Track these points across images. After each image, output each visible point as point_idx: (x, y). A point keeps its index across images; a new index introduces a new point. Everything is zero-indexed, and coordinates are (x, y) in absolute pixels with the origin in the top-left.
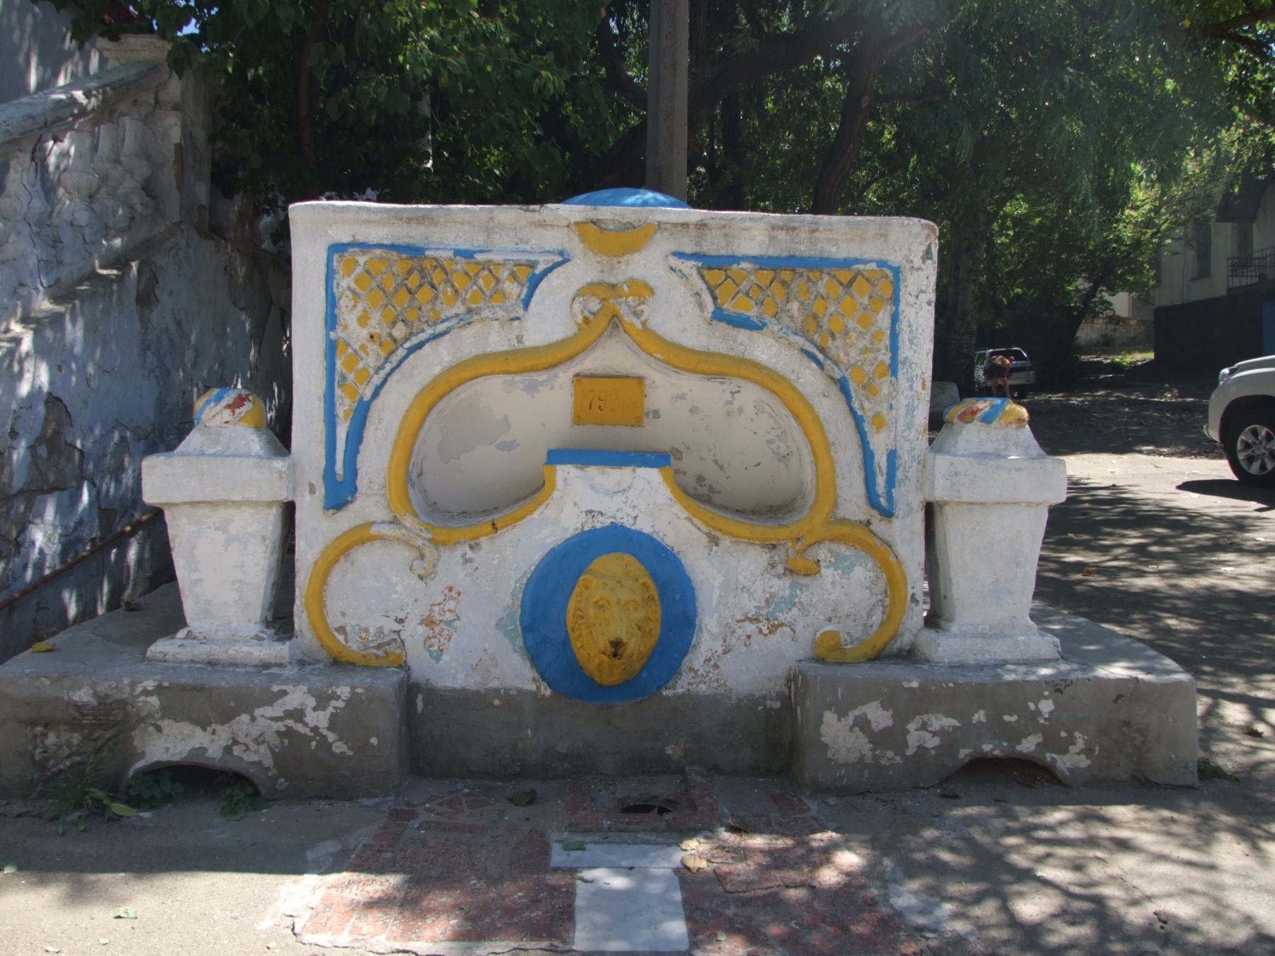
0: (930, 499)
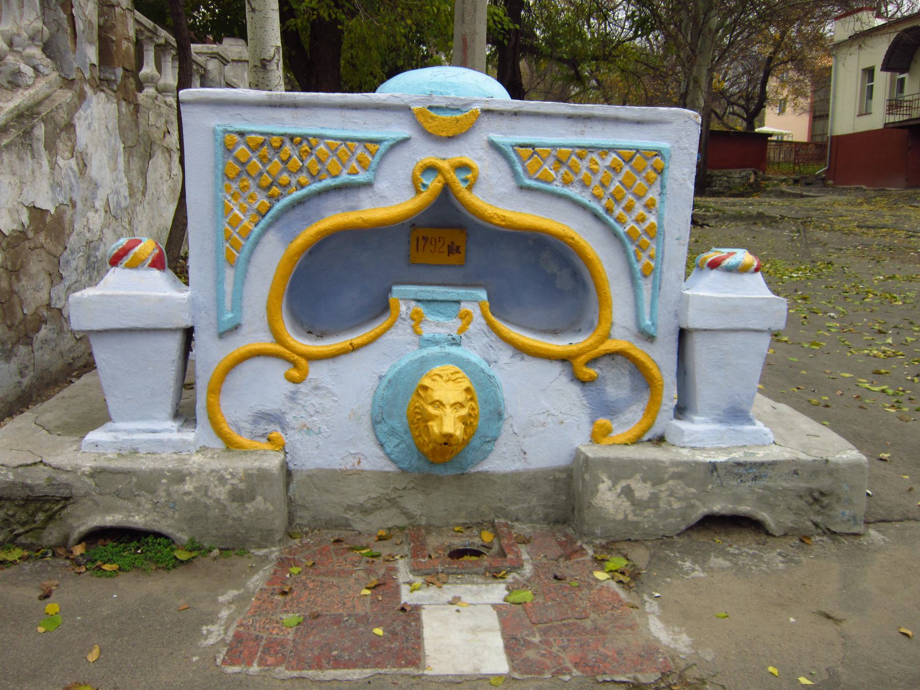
0: (684, 326)
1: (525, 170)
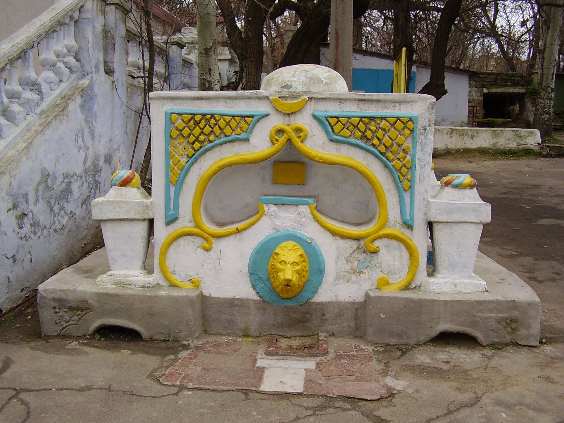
1: (333, 131)
